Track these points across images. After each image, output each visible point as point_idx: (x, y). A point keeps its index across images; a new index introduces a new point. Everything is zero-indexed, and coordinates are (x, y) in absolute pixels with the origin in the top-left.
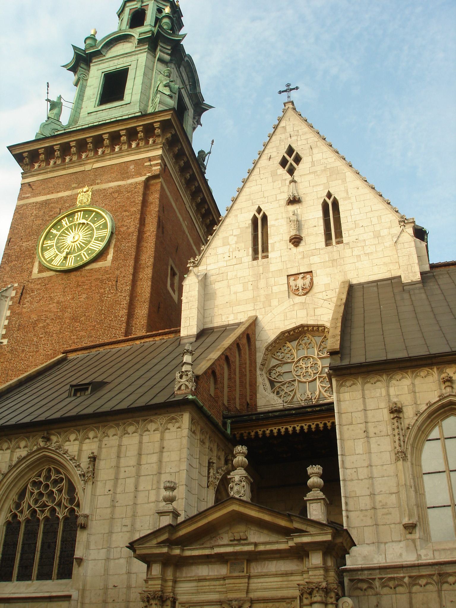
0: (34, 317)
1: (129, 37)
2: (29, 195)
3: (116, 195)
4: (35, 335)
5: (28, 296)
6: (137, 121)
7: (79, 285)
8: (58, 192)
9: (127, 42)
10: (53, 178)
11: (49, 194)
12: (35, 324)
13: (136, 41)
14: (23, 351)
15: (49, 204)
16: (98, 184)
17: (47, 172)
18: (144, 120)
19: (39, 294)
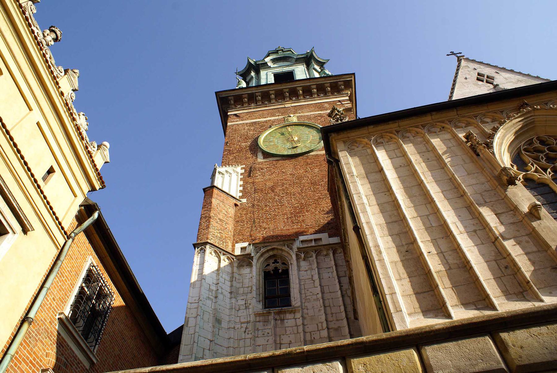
0: (270, 184)
1: (288, 58)
3: (319, 118)
5: (258, 172)
7: (307, 164)
8: (265, 118)
9: (286, 61)
11: (256, 119)
12: (272, 189)
13: (294, 60)
14: (266, 206)
16: (299, 113)
18: (331, 80)
19: (270, 171)
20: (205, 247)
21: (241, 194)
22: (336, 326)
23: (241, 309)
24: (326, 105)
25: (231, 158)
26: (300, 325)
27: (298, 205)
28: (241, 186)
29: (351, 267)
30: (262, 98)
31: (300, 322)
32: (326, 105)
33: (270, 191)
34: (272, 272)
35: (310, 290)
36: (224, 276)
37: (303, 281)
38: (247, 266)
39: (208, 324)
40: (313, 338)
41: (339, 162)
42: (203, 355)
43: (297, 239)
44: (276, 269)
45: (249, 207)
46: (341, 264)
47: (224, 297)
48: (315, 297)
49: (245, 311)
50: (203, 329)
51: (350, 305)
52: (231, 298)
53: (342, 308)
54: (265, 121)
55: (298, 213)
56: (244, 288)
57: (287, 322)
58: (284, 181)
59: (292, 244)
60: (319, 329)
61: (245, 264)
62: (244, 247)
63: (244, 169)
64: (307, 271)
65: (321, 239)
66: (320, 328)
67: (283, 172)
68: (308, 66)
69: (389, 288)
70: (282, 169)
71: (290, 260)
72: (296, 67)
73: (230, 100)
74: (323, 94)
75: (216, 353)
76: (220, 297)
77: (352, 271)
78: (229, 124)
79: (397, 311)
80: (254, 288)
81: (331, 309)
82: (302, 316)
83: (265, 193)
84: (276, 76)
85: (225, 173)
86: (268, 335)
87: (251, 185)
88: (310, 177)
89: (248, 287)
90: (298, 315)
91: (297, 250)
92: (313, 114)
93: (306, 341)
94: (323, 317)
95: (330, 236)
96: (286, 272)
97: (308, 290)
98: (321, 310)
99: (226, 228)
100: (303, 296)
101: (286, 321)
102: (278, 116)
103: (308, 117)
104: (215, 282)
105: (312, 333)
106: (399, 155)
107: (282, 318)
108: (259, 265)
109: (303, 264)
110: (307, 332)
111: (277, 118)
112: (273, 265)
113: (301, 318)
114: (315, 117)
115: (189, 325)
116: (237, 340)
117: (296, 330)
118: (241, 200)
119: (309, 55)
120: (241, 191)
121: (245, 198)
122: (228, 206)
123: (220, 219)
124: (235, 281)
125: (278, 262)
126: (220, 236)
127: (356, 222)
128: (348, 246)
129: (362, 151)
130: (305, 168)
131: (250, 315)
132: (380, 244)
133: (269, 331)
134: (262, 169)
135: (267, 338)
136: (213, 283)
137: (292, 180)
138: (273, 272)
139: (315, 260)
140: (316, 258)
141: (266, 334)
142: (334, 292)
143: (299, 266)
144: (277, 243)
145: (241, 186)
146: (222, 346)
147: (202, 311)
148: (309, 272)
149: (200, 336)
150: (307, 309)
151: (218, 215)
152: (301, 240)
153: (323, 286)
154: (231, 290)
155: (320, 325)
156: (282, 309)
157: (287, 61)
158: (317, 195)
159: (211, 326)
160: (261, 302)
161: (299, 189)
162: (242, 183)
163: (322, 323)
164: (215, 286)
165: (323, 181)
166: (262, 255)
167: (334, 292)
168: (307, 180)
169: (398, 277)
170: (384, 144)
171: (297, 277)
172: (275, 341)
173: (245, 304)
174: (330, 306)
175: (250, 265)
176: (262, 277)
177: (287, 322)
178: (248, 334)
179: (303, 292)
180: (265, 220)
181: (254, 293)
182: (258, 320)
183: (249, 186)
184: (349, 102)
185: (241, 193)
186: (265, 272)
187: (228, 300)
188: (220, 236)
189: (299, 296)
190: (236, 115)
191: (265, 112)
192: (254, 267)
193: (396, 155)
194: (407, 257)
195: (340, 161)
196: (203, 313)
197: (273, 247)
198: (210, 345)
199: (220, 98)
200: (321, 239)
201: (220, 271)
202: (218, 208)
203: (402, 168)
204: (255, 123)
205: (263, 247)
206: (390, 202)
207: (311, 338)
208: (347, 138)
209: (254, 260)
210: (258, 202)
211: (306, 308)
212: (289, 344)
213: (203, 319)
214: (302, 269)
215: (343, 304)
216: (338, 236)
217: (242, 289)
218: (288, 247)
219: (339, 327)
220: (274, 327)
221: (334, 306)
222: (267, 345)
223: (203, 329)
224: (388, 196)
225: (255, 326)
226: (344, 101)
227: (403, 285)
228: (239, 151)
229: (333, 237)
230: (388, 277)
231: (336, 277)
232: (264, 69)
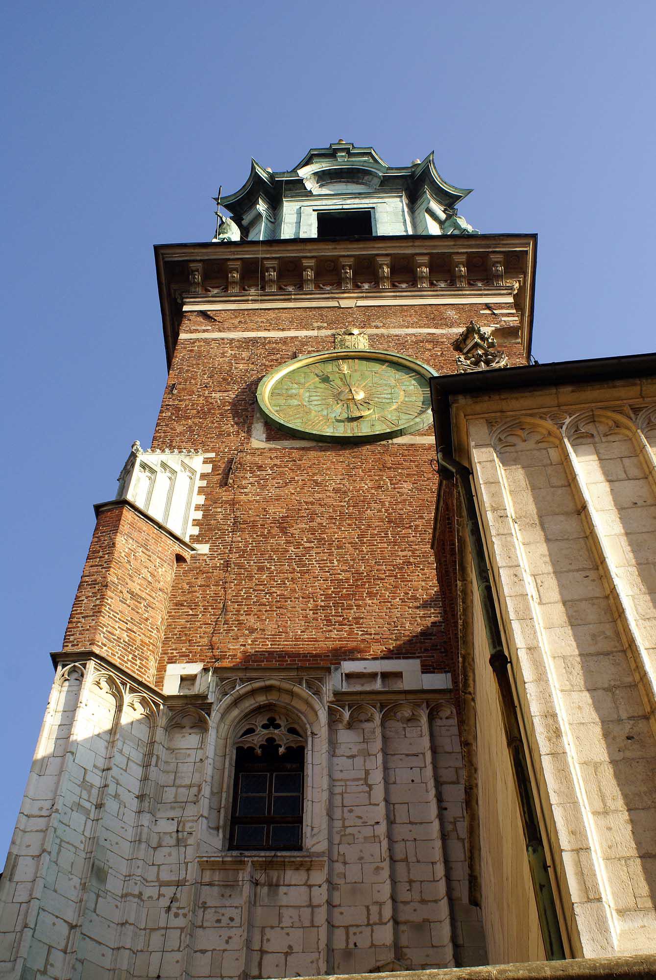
0: (277, 511)
1: (360, 175)
2: (210, 328)
3: (429, 346)
4: (288, 542)
5: (249, 475)
6: (454, 245)
7: (384, 467)
8: (283, 330)
10: (263, 311)
11: (258, 330)
12: (283, 525)
13: (376, 181)
14: (261, 569)
15: (264, 344)
16: (377, 327)
17: (248, 300)
18: (470, 246)
19: (282, 474)
20: (84, 666)
21: (196, 531)
22: (416, 918)
23: (164, 844)
24: (451, 313)
25: (179, 429)
26: (319, 906)
27: (348, 575)
28: (197, 508)
29: (474, 760)
30: (280, 276)
31: (320, 895)
32: (451, 313)
33: (275, 531)
34: (259, 751)
35: (358, 811)
36: (127, 750)
37: (343, 783)
38: (192, 728)
39: (70, 879)
40: (351, 946)
41: (471, 476)
42: (45, 967)
43: (336, 669)
44: (271, 745)
45: (215, 568)
46: (448, 748)
47: (122, 809)
48: (368, 831)
49: (174, 851)
50: (55, 891)
51: (460, 864)
52: (139, 812)
53: (440, 870)
54: (281, 339)
55: (347, 597)
56: (178, 787)
57: (285, 894)
58: (319, 509)
59: (320, 680)
60: (371, 922)
61: (186, 721)
62: (191, 675)
63: (210, 462)
64: (353, 757)
65: (401, 673)
66: (374, 918)
67: (316, 482)
68: (414, 200)
69: (573, 833)
70: (314, 474)
71: (311, 724)
72: (380, 200)
73: (193, 271)
74: (446, 281)
75: (83, 963)
76: (111, 805)
77: (476, 770)
78: (183, 336)
79: (589, 900)
80: (206, 791)
81: (409, 870)
82: (329, 881)
83: (262, 535)
84: (325, 220)
85: (158, 468)
86: (232, 924)
87: (226, 509)
88: (387, 504)
89: (190, 786)
90: (319, 877)
91: (331, 698)
92: (414, 335)
93: (333, 950)
94: (387, 889)
95: (426, 669)
96: (297, 755)
97: (351, 811)
98: (383, 869)
99: (147, 619)
100: (338, 824)
101: (283, 889)
102: (319, 328)
103: (398, 340)
104: (101, 763)
105: (352, 930)
106: (634, 472)
107: (275, 880)
108: (226, 727)
109: (346, 737)
110: (338, 927)
111: (314, 333)
112: (265, 731)
113: (325, 886)
114: (416, 343)
115: (16, 878)
116: (145, 929)
117: (309, 917)
118: (195, 546)
119: (419, 171)
120: (196, 523)
121: (207, 542)
122: (158, 560)
123: (131, 592)
124: (156, 765)
125: (278, 726)
126: (127, 639)
127: (500, 643)
128: (473, 704)
129: (535, 452)
130: (377, 478)
131: (187, 864)
132: (558, 711)
133: (234, 913)
134: (260, 468)
135: (226, 933)
136: (95, 766)
137: (338, 506)
138: (263, 752)
139: (378, 731)
140: (383, 724)
141: (225, 921)
142: (421, 823)
143: (333, 744)
144: (283, 674)
145: (197, 508)
146: (100, 943)
147: (58, 841)
148: (359, 761)
149: (44, 910)
150: (345, 863)
151: (129, 581)
152: (347, 672)
153: (394, 804)
154: (142, 788)
155: (374, 909)
156: (275, 856)
157: (358, 183)
158: (400, 553)
159: (78, 886)
160: (221, 831)
161: (355, 534)
162: (201, 500)
163: (381, 904)
164: (100, 774)
165: (421, 517)
166: (236, 703)
167: (421, 823)
168: (380, 511)
169: (599, 806)
170: (597, 439)
171: (325, 772)
172: (248, 942)
173: (178, 831)
174: (406, 860)
175: (201, 725)
176: (230, 764)
177: (285, 894)
178: (176, 915)
179: (338, 814)
180: (255, 609)
181: (204, 804)
182: (207, 878)
183: (219, 510)
184: (514, 311)
185: (198, 527)
186: (240, 750)
187: (130, 817)
188: (127, 639)
189: (325, 826)
190: (204, 314)
191: (284, 315)
192: (212, 734)
193: (625, 472)
194: (628, 754)
195: (472, 473)
196: (60, 845)
197: (268, 683)
198: (68, 938)
199: (166, 263)
200: (401, 673)
201: (118, 736)
202: (129, 562)
203: (639, 509)
204: (254, 341)
205: (241, 680)
206: (597, 598)
207: (347, 943)
208: (498, 414)
209: (213, 714)
210: (240, 557)
211: (341, 859)
212: (287, 954)
213: (56, 863)
214: (341, 750)
215: (442, 859)
216: (446, 672)
217: (174, 789)
218: (309, 686)
219: (427, 921)
220: (250, 902)
221: (418, 862)
222: (224, 951)
223: (55, 891)
224: (594, 580)
225: (197, 895)
226: (500, 306)
227: (609, 829)
228: (203, 414)
229: (433, 672)
230: (572, 803)
231: (431, 783)
232: (292, 197)
